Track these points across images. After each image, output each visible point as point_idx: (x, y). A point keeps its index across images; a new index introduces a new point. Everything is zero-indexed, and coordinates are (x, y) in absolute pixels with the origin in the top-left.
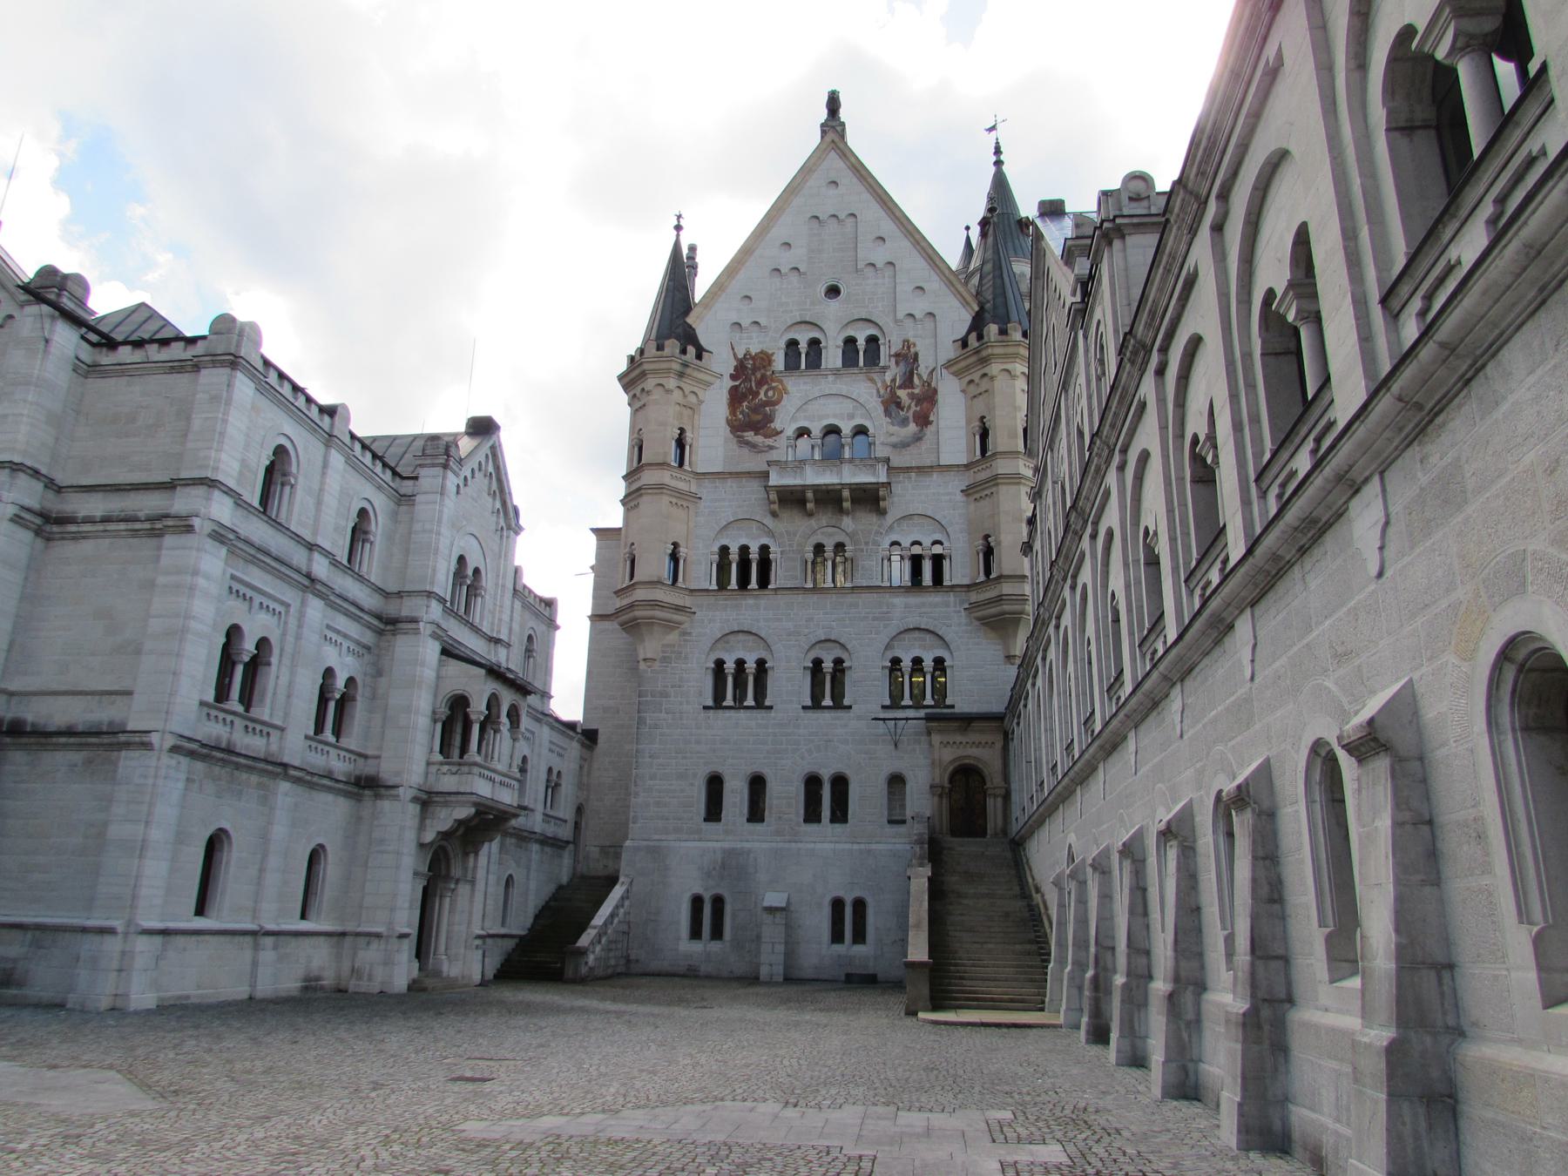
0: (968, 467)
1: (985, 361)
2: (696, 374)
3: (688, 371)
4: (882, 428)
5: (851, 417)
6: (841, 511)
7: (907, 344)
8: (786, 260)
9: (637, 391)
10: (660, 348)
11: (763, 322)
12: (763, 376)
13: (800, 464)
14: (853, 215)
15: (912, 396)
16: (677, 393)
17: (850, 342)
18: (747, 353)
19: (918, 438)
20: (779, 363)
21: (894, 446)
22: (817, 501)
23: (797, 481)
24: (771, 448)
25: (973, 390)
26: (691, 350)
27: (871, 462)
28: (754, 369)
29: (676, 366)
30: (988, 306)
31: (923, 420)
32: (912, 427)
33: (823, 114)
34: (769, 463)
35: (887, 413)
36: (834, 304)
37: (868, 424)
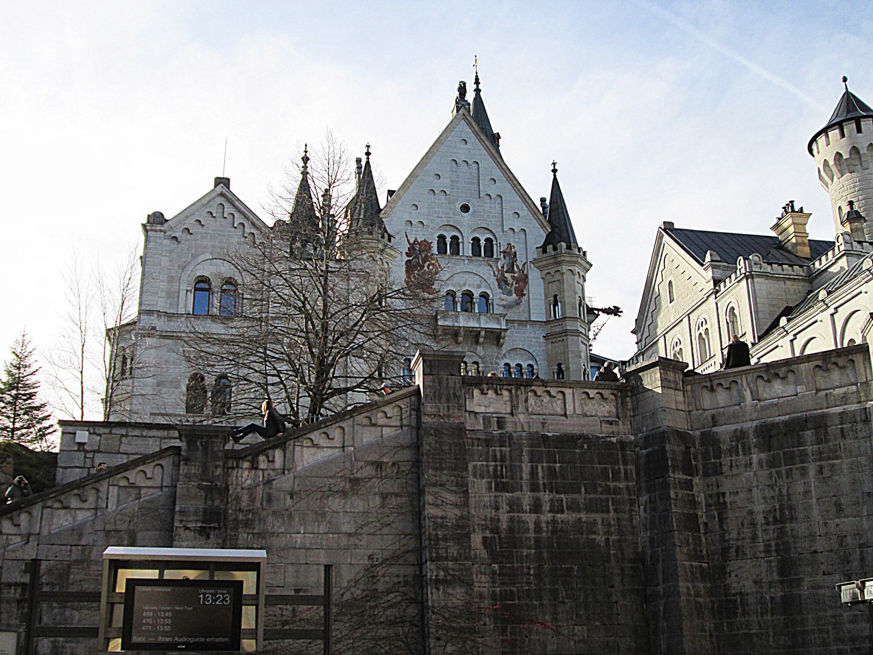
1: (559, 263)
4: (497, 296)
5: (479, 286)
6: (477, 342)
12: (426, 256)
14: (477, 163)
15: (513, 277)
16: (379, 262)
17: (476, 240)
18: (416, 240)
19: (518, 303)
20: (435, 250)
21: (504, 306)
24: (433, 300)
25: (549, 276)
26: (386, 235)
27: (498, 318)
28: (421, 251)
30: (556, 230)
31: (520, 293)
33: (457, 94)
35: (500, 287)
37: (489, 292)
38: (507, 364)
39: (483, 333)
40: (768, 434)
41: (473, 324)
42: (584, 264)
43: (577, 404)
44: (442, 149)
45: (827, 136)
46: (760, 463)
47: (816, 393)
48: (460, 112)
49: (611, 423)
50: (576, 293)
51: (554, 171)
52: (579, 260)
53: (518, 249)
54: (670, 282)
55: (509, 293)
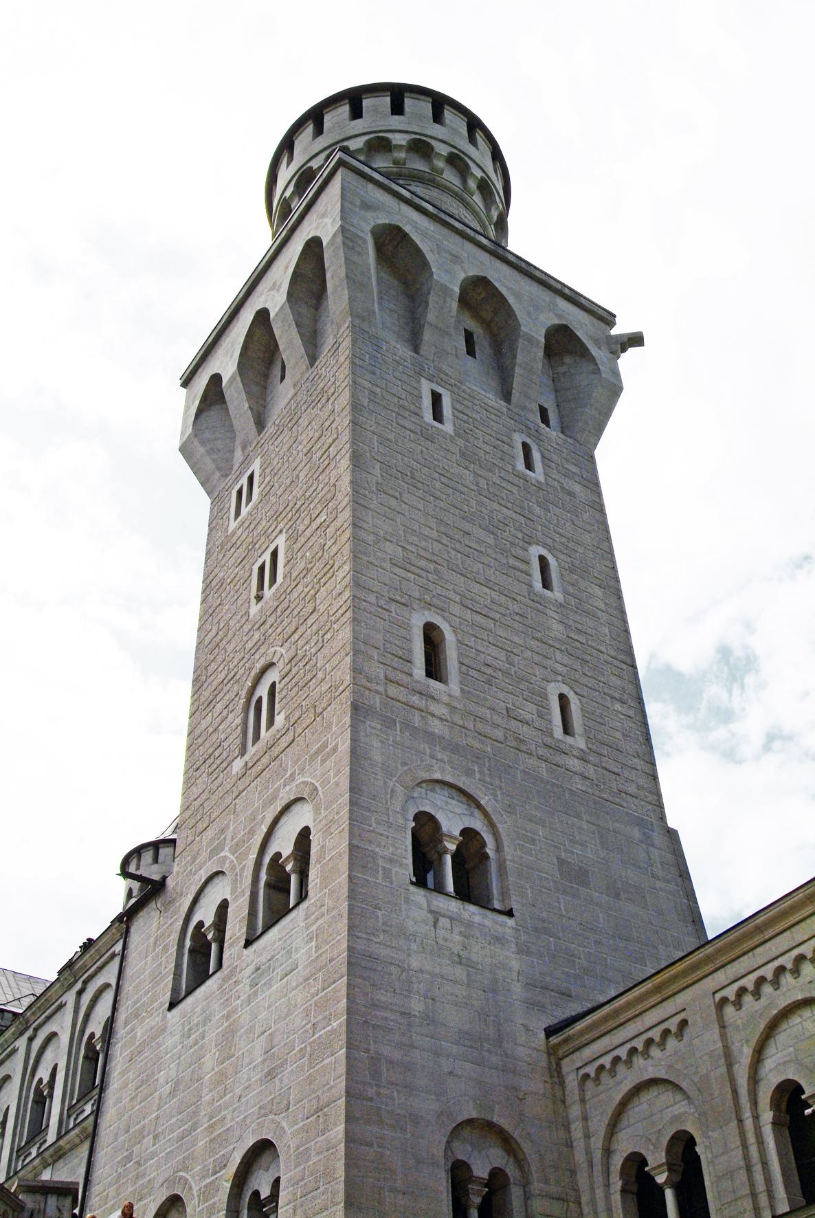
45: (139, 860)
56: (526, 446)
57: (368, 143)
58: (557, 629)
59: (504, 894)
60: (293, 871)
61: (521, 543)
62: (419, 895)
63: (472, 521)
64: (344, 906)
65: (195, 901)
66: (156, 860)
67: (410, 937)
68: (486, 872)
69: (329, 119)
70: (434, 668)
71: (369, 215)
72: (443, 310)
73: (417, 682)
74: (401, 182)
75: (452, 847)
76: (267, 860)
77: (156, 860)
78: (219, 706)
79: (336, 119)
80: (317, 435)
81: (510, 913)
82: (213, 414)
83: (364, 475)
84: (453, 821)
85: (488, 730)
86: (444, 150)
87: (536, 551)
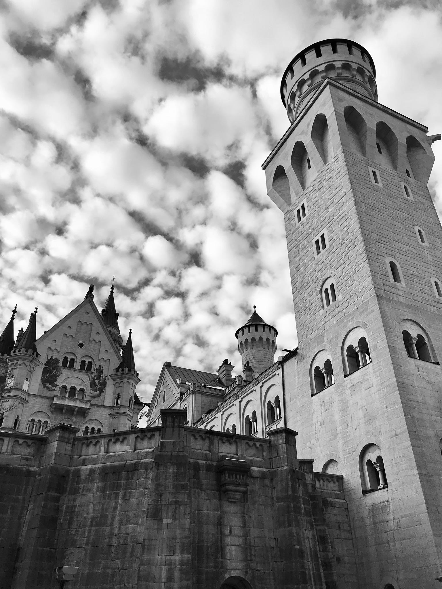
0: (112, 407)
1: (123, 378)
2: (35, 362)
3: (34, 361)
5: (80, 385)
7: (100, 366)
8: (69, 332)
9: (15, 363)
10: (27, 351)
11: (59, 349)
12: (55, 366)
13: (64, 398)
16: (29, 367)
17: (83, 362)
18: (52, 357)
19: (99, 396)
20: (61, 364)
21: (91, 397)
22: (67, 410)
23: (62, 403)
24: (54, 390)
25: (117, 384)
28: (53, 364)
29: (31, 359)
30: (125, 361)
31: (101, 391)
32: (98, 392)
33: (88, 290)
34: (54, 396)
35: (91, 387)
36: (81, 349)
37: (85, 388)
38: (87, 428)
39: (76, 409)
40: (105, 472)
41: (72, 404)
42: (136, 379)
43: (10, 446)
44: (76, 315)
45: (243, 331)
46: (98, 487)
47: (134, 451)
48: (88, 299)
49: (27, 459)
50: (129, 394)
51: (130, 333)
52: (133, 377)
53: (105, 369)
54: (165, 392)
55: (96, 390)
56: (405, 187)
57: (326, 67)
58: (429, 258)
59: (435, 357)
60: (359, 351)
61: (412, 226)
62: (411, 360)
63: (395, 220)
64: (392, 367)
65: (313, 359)
66: (249, 331)
67: (412, 375)
68: (427, 349)
69: (308, 57)
70: (396, 278)
71: (342, 104)
72: (371, 139)
73: (392, 284)
74: (340, 82)
75: (415, 342)
76: (346, 347)
77: (249, 331)
78: (307, 291)
79: (310, 56)
80: (334, 192)
81: (438, 364)
82: (280, 182)
83: (361, 209)
84: (414, 332)
85: (416, 298)
86: (355, 66)
87: (417, 228)
